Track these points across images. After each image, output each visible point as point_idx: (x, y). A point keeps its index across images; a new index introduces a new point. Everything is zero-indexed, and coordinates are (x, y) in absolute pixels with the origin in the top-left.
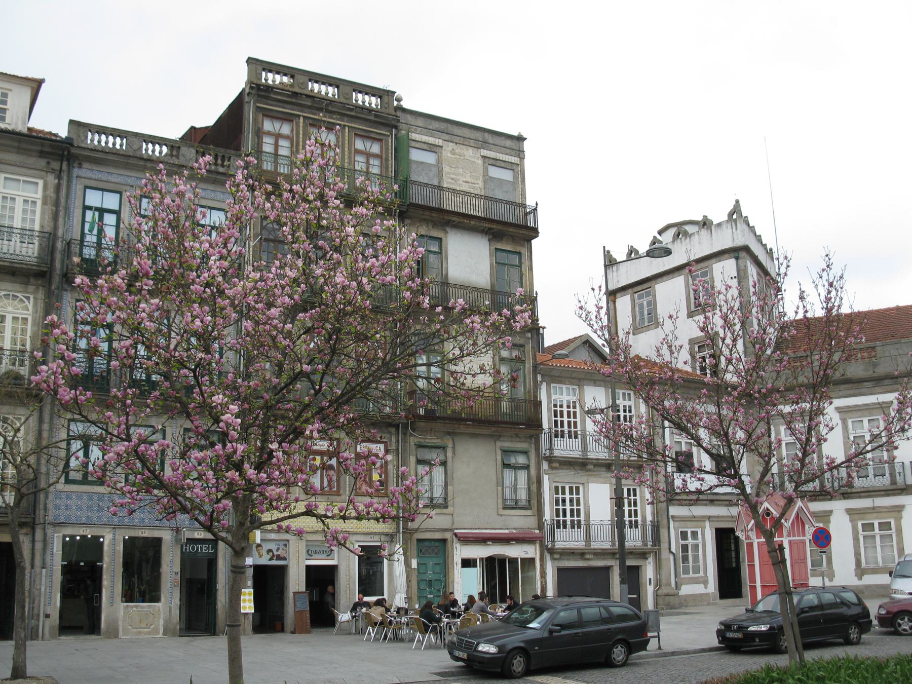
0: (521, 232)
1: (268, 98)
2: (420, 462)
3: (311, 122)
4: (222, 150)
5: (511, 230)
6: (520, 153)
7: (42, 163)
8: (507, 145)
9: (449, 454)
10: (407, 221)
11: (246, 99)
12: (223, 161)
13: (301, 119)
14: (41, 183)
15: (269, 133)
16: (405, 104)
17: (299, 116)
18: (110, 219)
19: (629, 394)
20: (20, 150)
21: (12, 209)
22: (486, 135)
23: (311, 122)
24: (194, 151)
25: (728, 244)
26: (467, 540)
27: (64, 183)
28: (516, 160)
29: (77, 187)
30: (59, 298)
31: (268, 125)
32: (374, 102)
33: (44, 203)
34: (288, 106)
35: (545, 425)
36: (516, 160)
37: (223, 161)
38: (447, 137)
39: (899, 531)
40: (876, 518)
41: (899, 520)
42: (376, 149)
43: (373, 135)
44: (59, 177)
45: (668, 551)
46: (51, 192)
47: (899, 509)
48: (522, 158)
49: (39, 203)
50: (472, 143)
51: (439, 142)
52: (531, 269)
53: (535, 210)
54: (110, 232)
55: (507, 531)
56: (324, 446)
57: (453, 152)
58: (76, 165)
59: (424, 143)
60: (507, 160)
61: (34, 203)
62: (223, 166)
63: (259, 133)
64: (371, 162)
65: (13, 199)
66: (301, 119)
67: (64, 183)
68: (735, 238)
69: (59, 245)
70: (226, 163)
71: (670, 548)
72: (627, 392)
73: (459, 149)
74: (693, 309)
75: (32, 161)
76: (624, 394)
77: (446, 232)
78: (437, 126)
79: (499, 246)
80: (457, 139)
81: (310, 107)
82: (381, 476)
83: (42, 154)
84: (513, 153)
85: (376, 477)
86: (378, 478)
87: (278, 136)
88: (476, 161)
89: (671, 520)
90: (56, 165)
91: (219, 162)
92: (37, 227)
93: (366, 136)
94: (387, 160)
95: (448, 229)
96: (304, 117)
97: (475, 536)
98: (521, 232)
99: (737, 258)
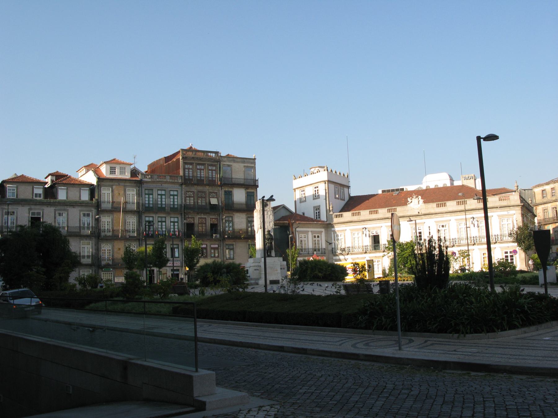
6: (255, 163)
7: (135, 184)
9: (234, 246)
14: (135, 190)
15: (187, 169)
16: (222, 155)
20: (130, 183)
21: (130, 197)
27: (140, 189)
28: (253, 165)
29: (143, 190)
30: (141, 216)
32: (213, 155)
33: (136, 194)
36: (253, 165)
42: (214, 168)
44: (139, 188)
46: (138, 192)
48: (255, 165)
49: (135, 195)
52: (257, 196)
53: (258, 180)
67: (140, 189)
74: (315, 197)
75: (133, 184)
77: (233, 189)
83: (135, 183)
90: (139, 185)
93: (212, 165)
94: (217, 171)
96: (196, 163)
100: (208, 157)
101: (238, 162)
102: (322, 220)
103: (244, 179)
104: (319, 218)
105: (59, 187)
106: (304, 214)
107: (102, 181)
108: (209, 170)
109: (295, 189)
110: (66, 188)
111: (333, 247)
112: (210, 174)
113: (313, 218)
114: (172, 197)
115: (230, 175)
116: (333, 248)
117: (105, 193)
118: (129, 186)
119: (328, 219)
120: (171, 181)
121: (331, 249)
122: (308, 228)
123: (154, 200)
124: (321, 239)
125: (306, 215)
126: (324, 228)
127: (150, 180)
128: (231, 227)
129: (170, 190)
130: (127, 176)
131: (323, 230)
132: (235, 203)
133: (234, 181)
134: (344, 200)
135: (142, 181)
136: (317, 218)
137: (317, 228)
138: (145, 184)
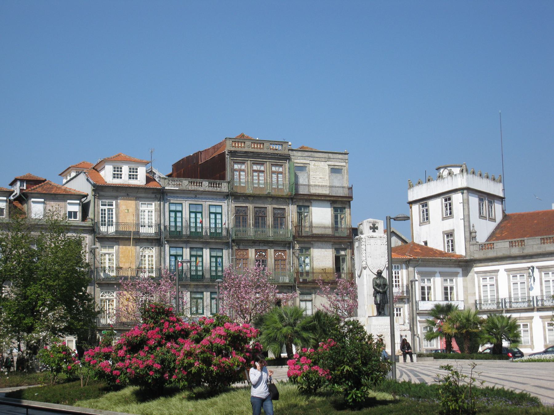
1: (235, 155)
2: (301, 301)
3: (253, 162)
4: (219, 181)
7: (153, 196)
8: (340, 158)
10: (294, 200)
11: (227, 156)
12: (219, 185)
13: (249, 162)
15: (236, 170)
17: (248, 160)
18: (179, 215)
19: (398, 266)
22: (330, 154)
23: (253, 162)
24: (208, 183)
25: (459, 186)
31: (236, 167)
33: (155, 211)
37: (219, 185)
38: (311, 159)
39: (531, 328)
40: (522, 323)
41: (531, 323)
43: (279, 164)
47: (531, 318)
49: (154, 211)
50: (323, 160)
51: (307, 162)
54: (179, 220)
57: (314, 165)
58: (165, 195)
61: (152, 212)
62: (219, 187)
63: (233, 170)
64: (279, 175)
65: (144, 211)
66: (249, 162)
68: (462, 182)
69: (162, 227)
70: (220, 186)
72: (396, 265)
73: (317, 163)
74: (444, 216)
75: (149, 196)
76: (395, 266)
79: (335, 206)
80: (316, 159)
83: (153, 193)
84: (342, 161)
87: (240, 170)
88: (325, 167)
89: (418, 322)
91: (217, 185)
92: (154, 222)
93: (276, 165)
94: (285, 174)
95: (312, 201)
99: (463, 193)
100: (272, 151)
101: (319, 160)
102: (457, 253)
103: (331, 187)
104: (453, 250)
105: (33, 200)
106: (426, 243)
107: (102, 191)
108: (273, 172)
109: (411, 203)
110: (43, 200)
111: (477, 298)
112: (274, 179)
113: (443, 250)
114: (213, 216)
115: (307, 180)
116: (476, 301)
117: (105, 210)
118: (143, 198)
119: (468, 251)
120: (211, 189)
121: (474, 302)
122: (435, 266)
123: (184, 220)
124: (457, 286)
125: (429, 245)
126: (460, 266)
127: (178, 189)
128: (307, 264)
129: (210, 205)
130: (141, 181)
131: (460, 270)
132: (314, 225)
133: (313, 191)
134: (494, 220)
135: (164, 190)
136: (448, 250)
137: (450, 267)
138: (169, 195)
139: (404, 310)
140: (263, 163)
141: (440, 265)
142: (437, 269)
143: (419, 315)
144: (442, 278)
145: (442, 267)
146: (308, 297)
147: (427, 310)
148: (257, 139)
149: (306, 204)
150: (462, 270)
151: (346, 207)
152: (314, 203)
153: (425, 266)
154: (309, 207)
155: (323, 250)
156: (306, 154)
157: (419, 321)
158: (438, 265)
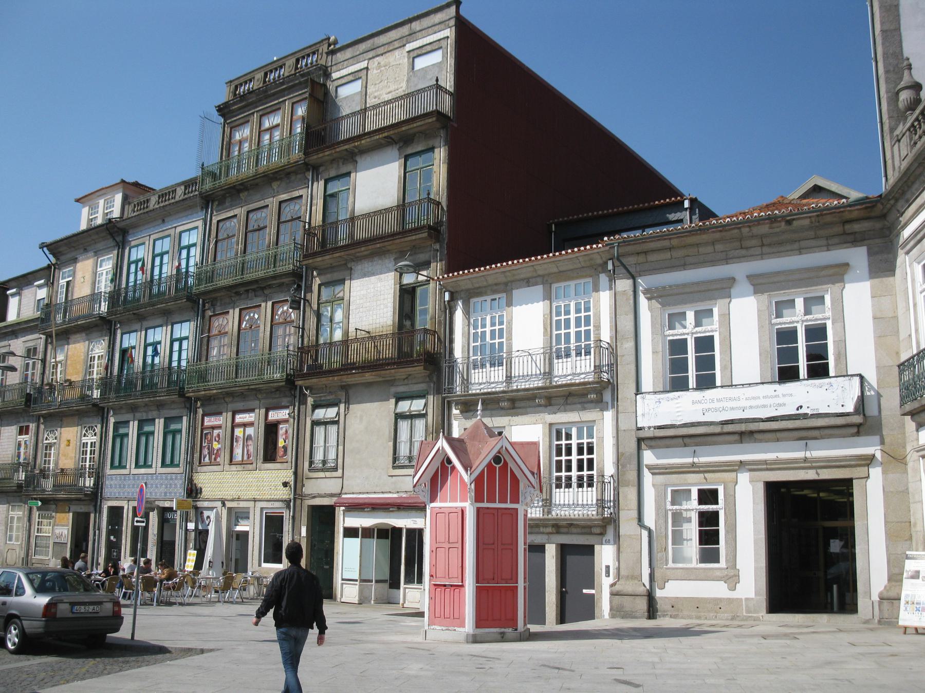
0: (415, 125)
5: (404, 129)
26: (355, 507)
34: (246, 109)
35: (458, 353)
38: (371, 54)
45: (636, 521)
55: (395, 496)
56: (246, 418)
59: (349, 74)
60: (431, 41)
71: (640, 519)
78: (364, 47)
81: (260, 100)
82: (285, 442)
84: (442, 26)
85: (281, 444)
86: (283, 444)
89: (646, 473)
97: (350, 501)
98: (415, 125)
122: (727, 260)
126: (855, 240)
131: (858, 256)
138: (131, 232)
139: (601, 431)
140: (278, 106)
141: (752, 251)
142: (739, 270)
143: (650, 447)
144: (764, 297)
145: (762, 256)
146: (331, 413)
147: (672, 426)
148: (275, 59)
149: (344, 170)
150: (870, 254)
151: (436, 144)
152: (361, 161)
153: (684, 266)
154: (348, 174)
155: (373, 278)
156: (362, 47)
157: (650, 468)
158: (743, 252)
